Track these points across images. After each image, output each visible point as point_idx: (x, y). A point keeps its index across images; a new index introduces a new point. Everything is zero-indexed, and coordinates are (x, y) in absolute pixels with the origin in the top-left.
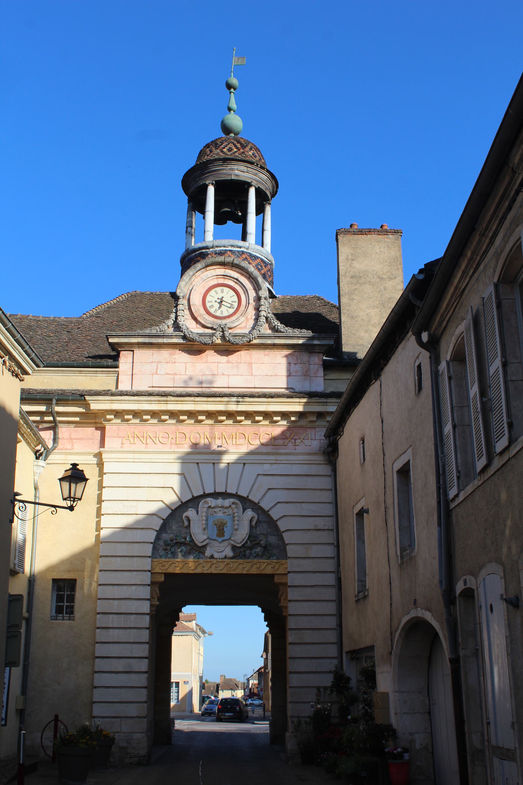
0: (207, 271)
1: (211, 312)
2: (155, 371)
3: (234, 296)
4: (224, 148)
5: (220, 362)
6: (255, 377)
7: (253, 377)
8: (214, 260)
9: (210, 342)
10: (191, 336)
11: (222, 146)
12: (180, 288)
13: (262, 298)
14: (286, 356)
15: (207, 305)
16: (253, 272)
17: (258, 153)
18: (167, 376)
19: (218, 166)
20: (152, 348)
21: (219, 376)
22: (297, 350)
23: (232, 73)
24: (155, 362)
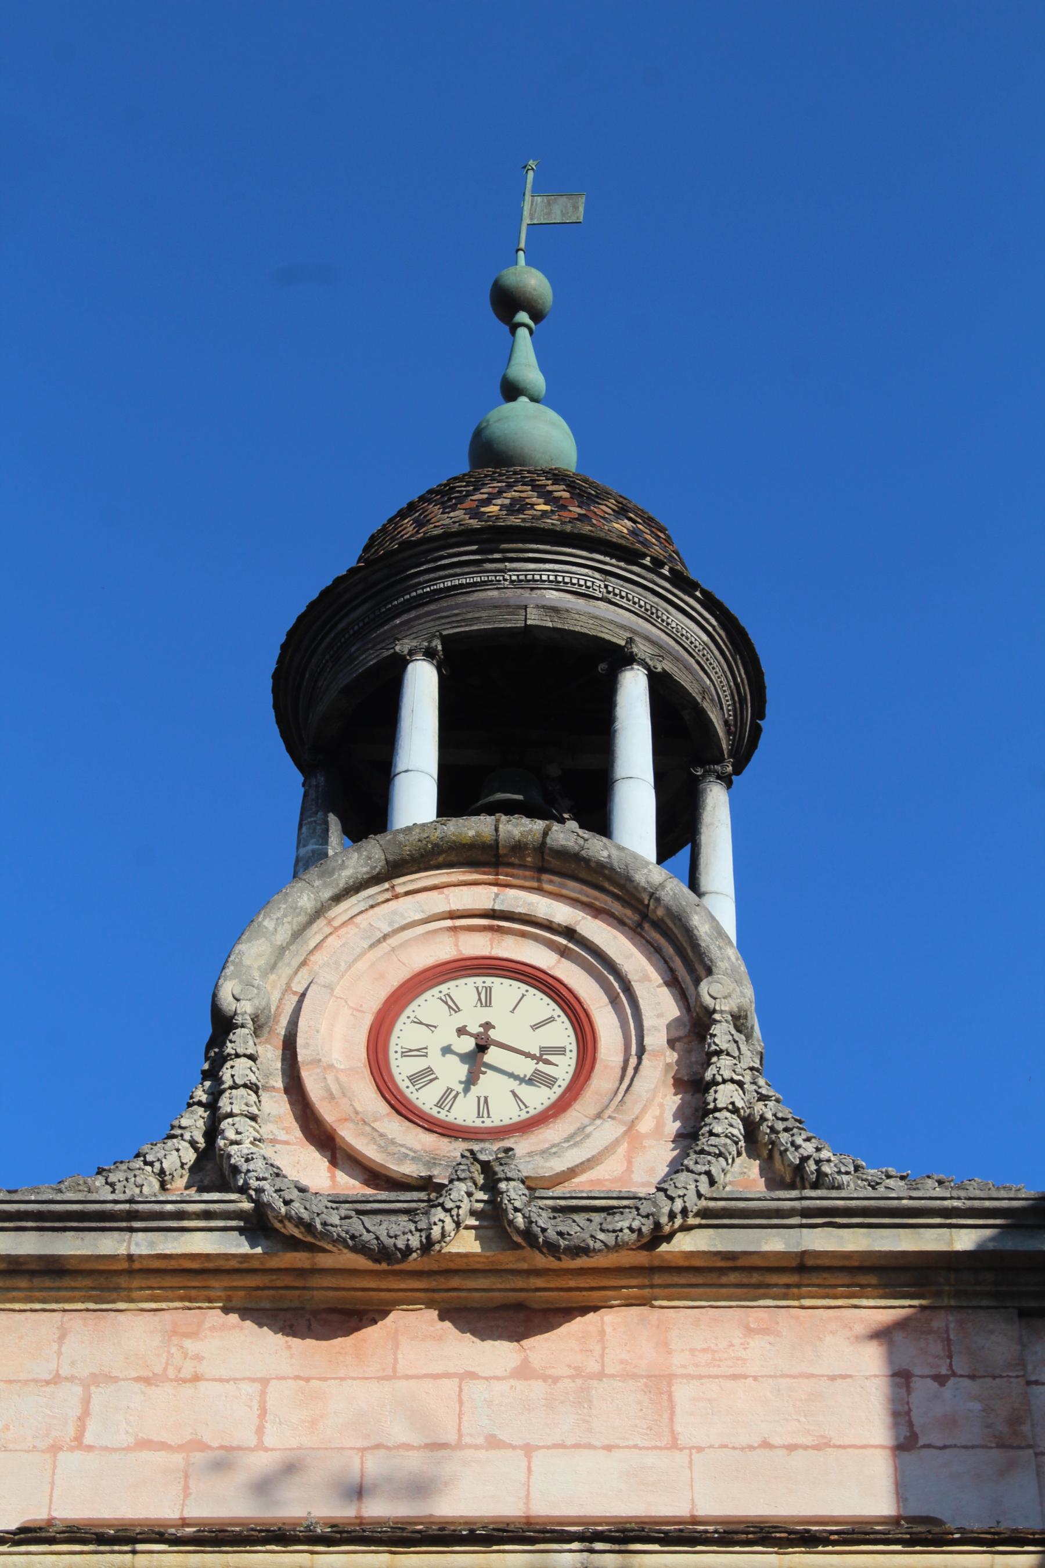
0: (397, 897)
1: (419, 1103)
2: (71, 1431)
3: (551, 1019)
4: (487, 502)
5: (472, 1376)
6: (696, 1456)
7: (681, 1457)
8: (438, 834)
9: (415, 1241)
10: (298, 1208)
11: (478, 497)
12: (234, 976)
13: (717, 1016)
14: (882, 1335)
15: (395, 1071)
16: (662, 886)
17: (658, 538)
18: (145, 1455)
19: (458, 570)
20: (57, 1301)
21: (469, 1453)
22: (945, 1302)
23: (521, 253)
24: (71, 1379)
